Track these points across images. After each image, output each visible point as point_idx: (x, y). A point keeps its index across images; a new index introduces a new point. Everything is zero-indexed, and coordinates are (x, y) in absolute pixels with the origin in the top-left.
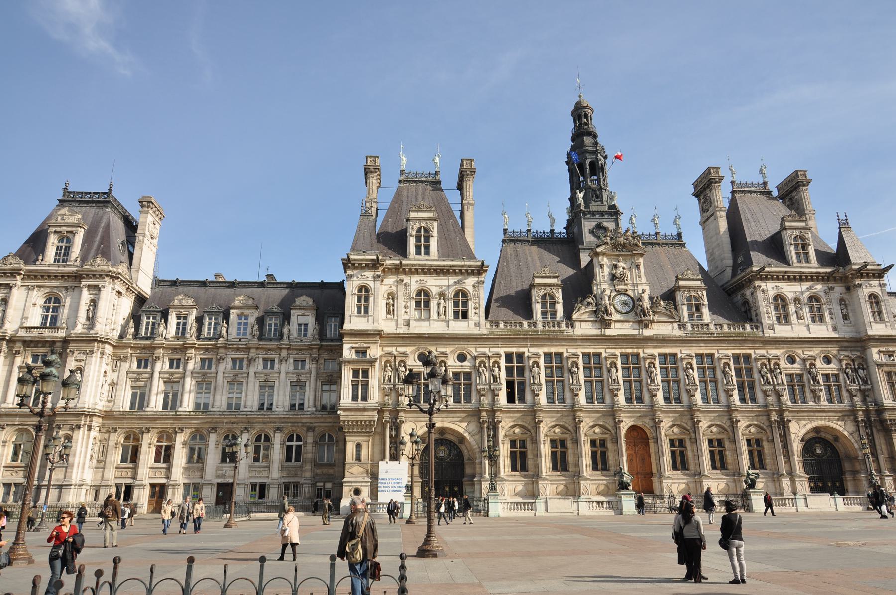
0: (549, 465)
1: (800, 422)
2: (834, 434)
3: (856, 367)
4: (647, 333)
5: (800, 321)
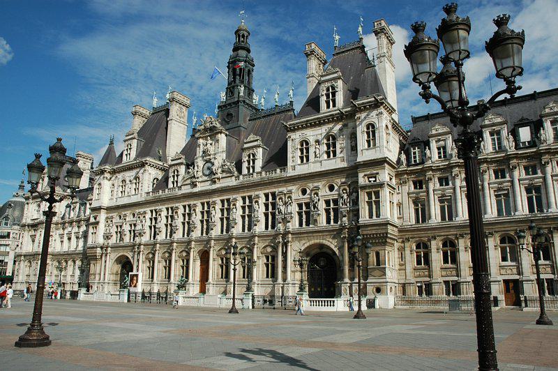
4: (215, 187)
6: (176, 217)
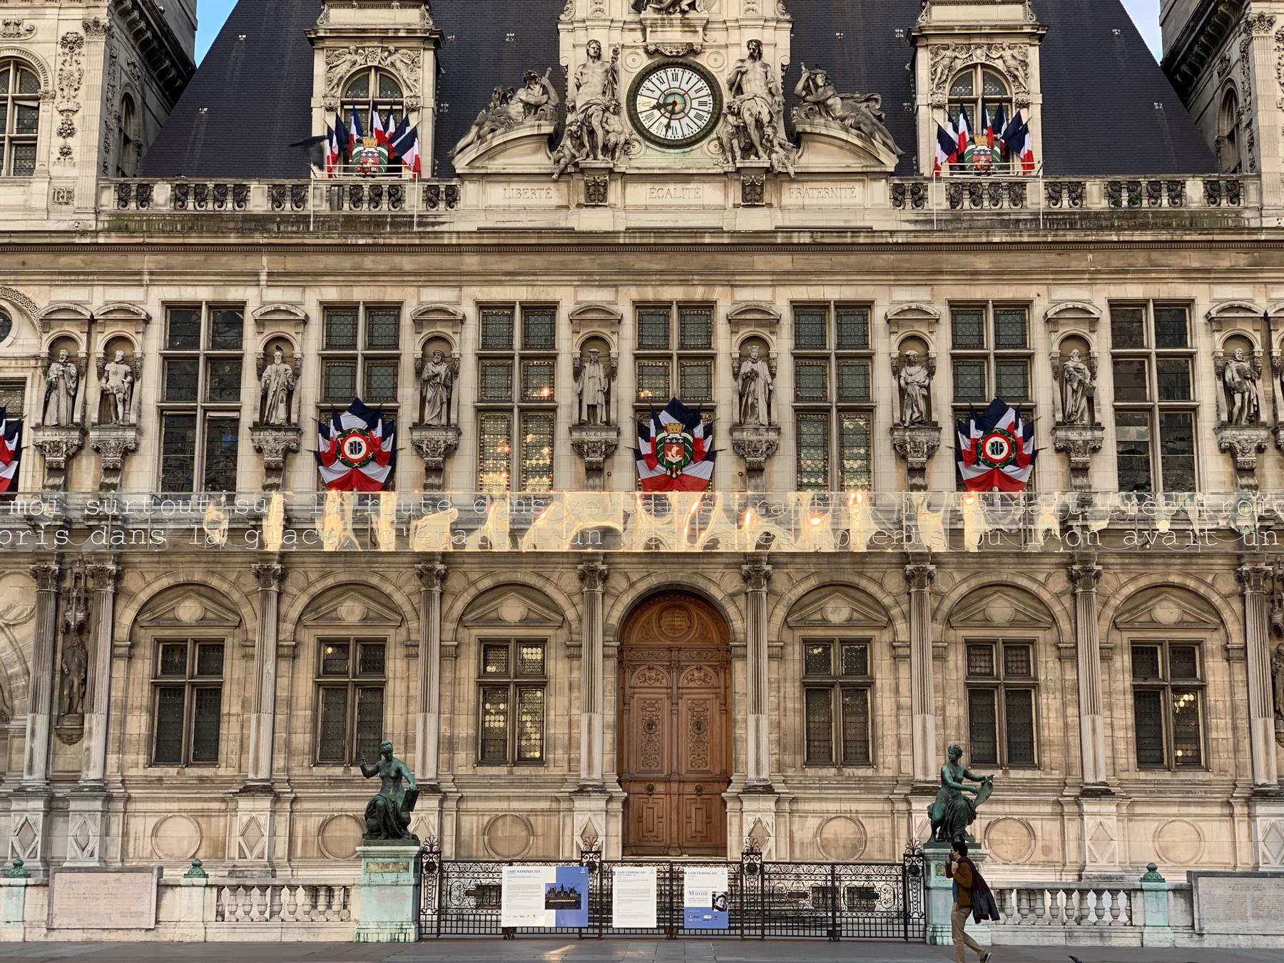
0: (302, 740)
4: (756, 220)
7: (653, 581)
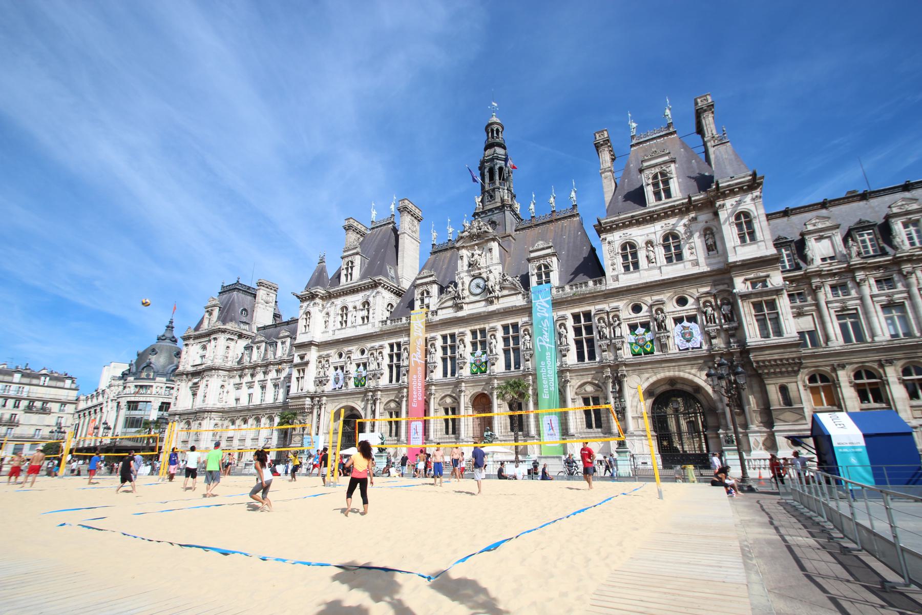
1: (641, 375)
2: (694, 385)
3: (719, 302)
4: (492, 308)
5: (651, 265)
6: (433, 350)
7: (475, 391)
